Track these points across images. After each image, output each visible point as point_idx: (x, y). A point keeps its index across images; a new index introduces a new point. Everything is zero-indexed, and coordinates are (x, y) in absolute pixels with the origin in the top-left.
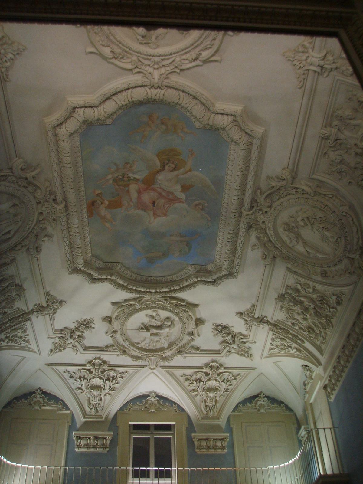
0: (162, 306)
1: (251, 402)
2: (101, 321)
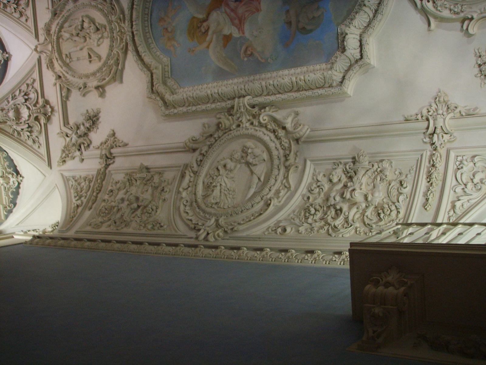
1: (9, 167)
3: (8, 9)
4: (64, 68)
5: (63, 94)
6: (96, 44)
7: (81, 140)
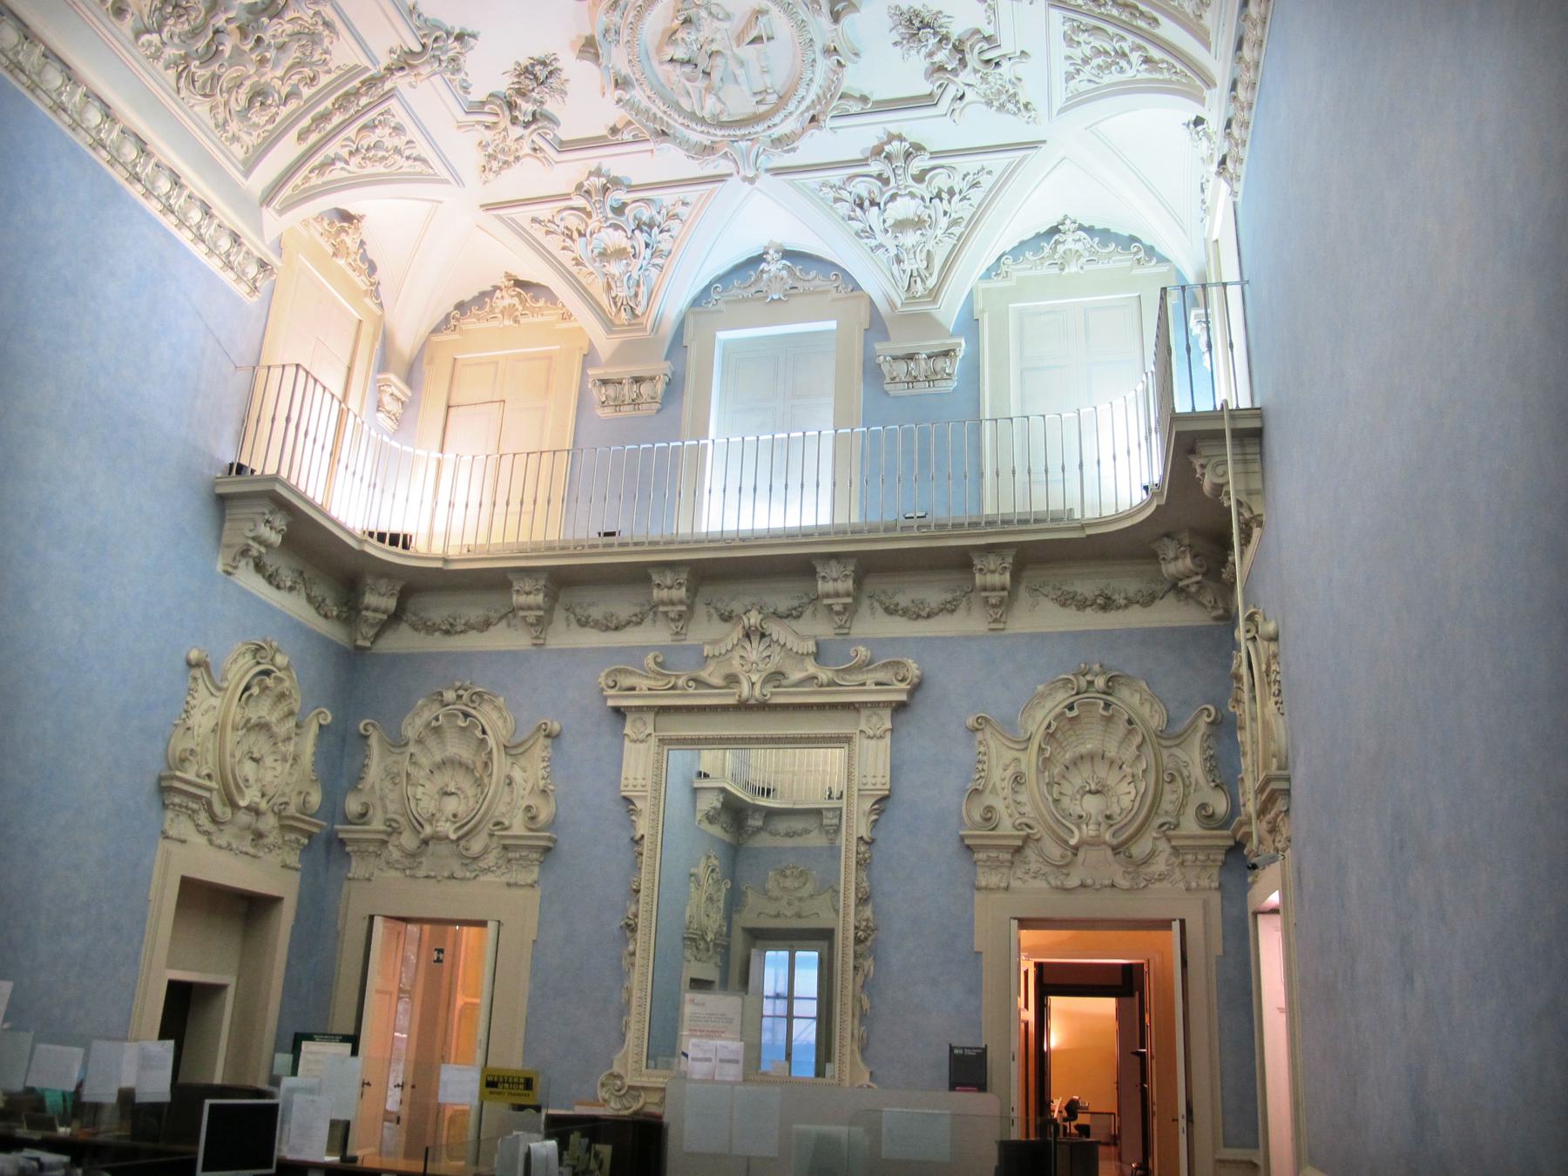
3: (665, 246)
4: (791, 107)
6: (726, 25)
7: (973, 60)
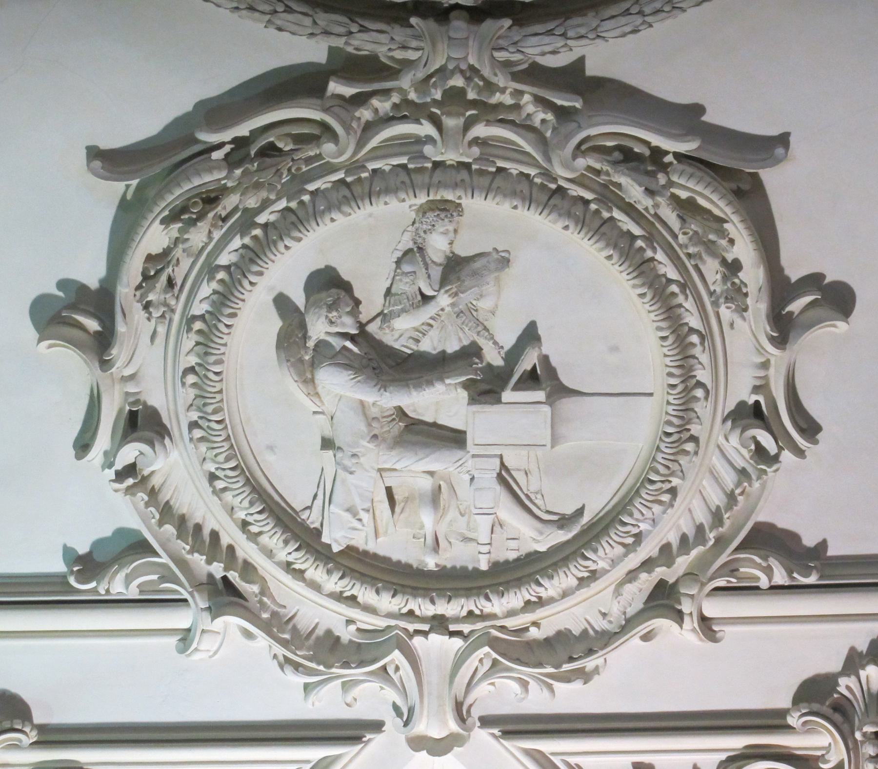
0: (514, 168)
2: (31, 333)
5: (780, 577)
